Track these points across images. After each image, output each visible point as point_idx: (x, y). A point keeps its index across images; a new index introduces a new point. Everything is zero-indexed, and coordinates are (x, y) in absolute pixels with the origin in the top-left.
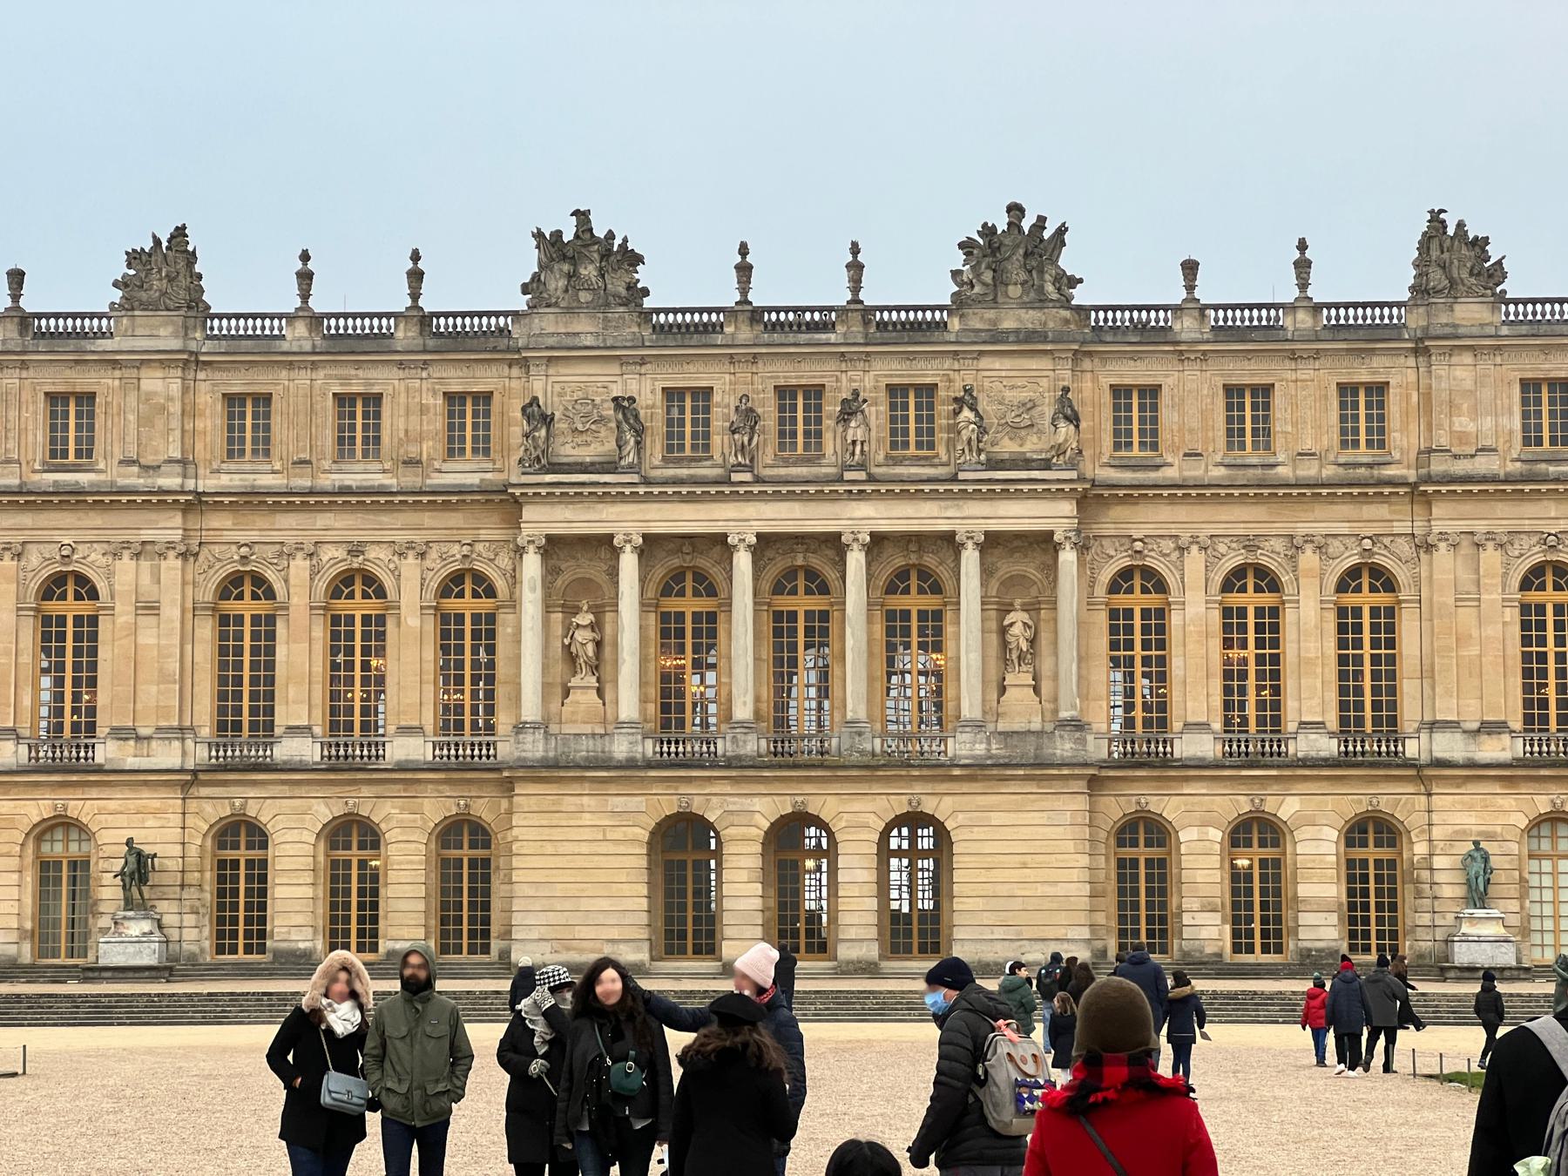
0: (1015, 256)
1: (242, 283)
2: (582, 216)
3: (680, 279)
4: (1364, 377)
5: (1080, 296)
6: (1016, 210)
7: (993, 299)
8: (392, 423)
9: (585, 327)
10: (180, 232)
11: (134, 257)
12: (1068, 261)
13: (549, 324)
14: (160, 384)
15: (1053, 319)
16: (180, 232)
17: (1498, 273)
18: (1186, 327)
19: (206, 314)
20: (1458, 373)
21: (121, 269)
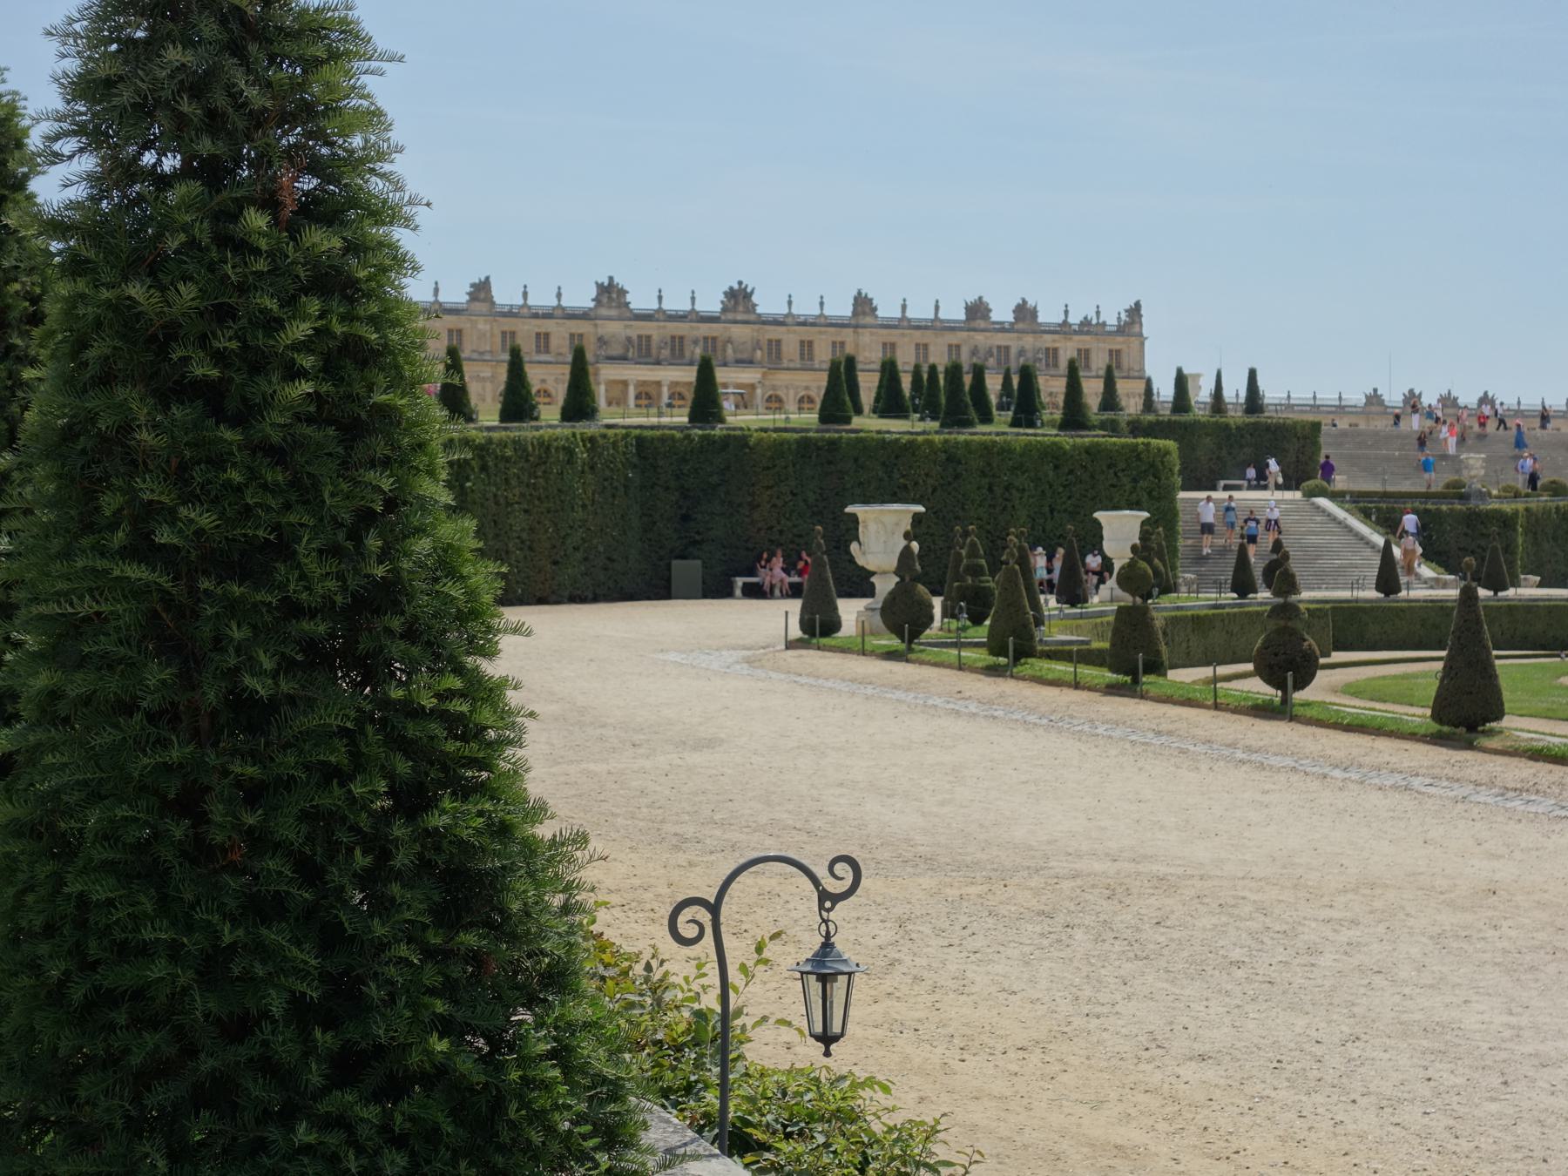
0: (739, 297)
1: (504, 295)
2: (611, 279)
3: (640, 300)
4: (839, 339)
5: (759, 310)
6: (740, 283)
7: (734, 309)
8: (554, 342)
9: (613, 313)
10: (487, 278)
11: (473, 285)
12: (755, 299)
13: (604, 312)
14: (483, 325)
15: (752, 317)
16: (487, 278)
17: (875, 309)
18: (789, 320)
19: (493, 303)
20: (866, 337)
21: (469, 289)
